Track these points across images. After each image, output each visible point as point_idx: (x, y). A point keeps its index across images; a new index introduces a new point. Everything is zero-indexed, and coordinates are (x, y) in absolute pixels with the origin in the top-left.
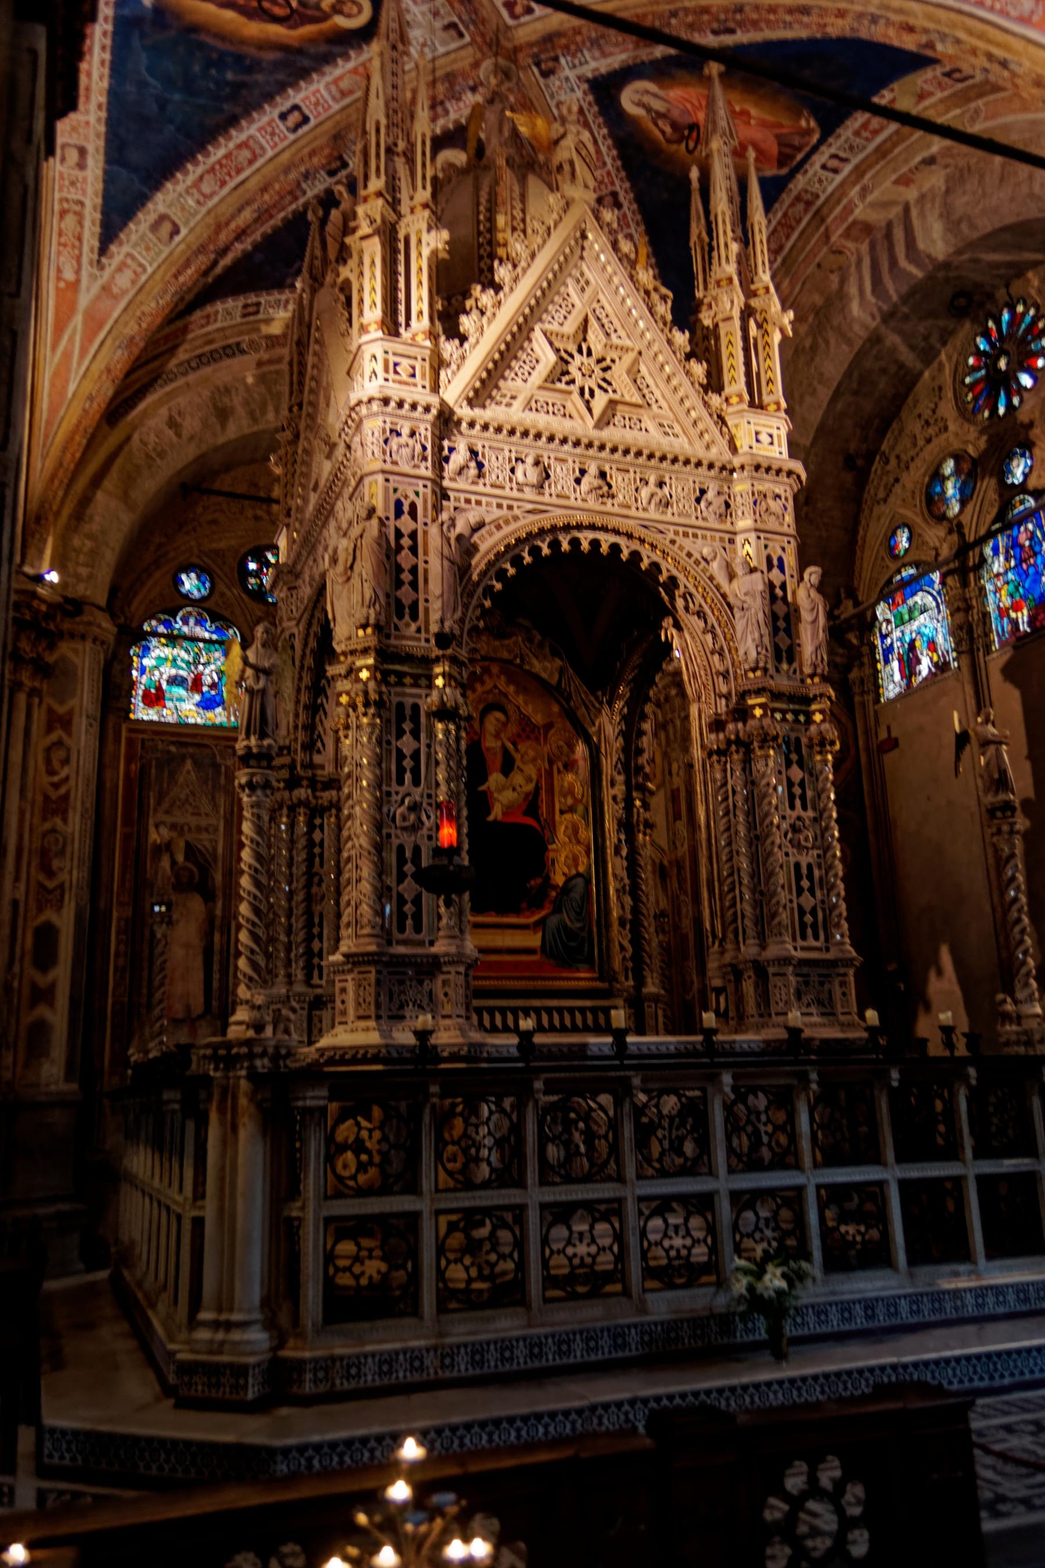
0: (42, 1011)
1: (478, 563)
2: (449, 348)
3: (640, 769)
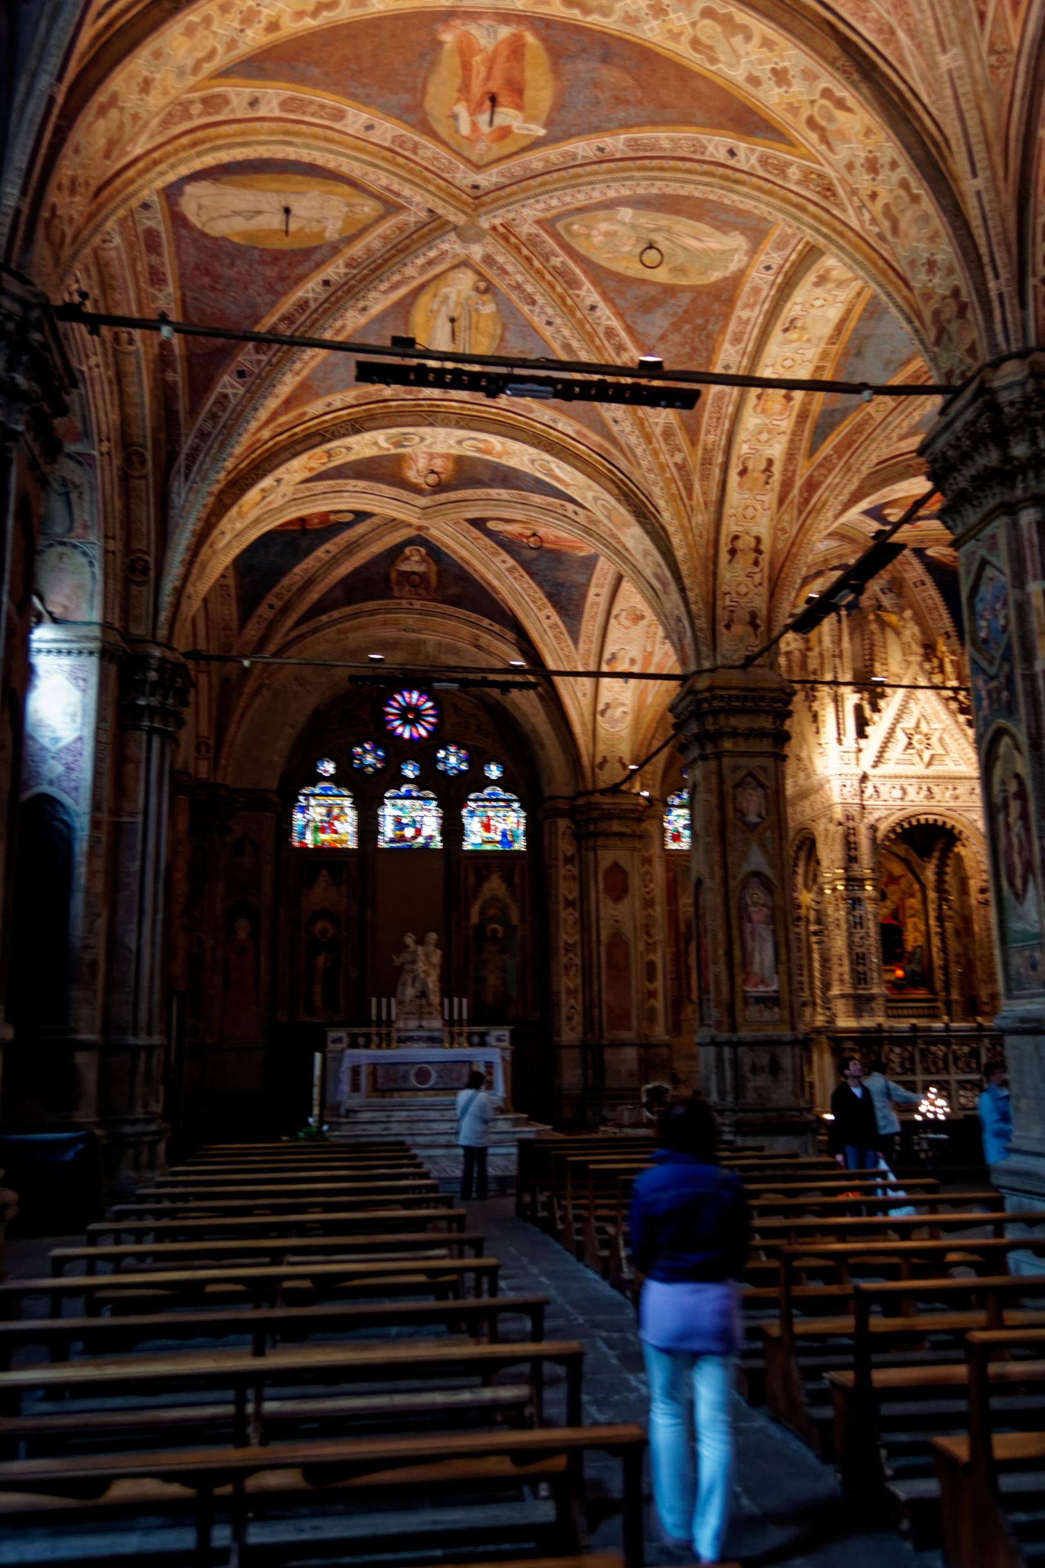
0: (653, 1002)
1: (880, 835)
2: (862, 742)
3: (946, 891)
